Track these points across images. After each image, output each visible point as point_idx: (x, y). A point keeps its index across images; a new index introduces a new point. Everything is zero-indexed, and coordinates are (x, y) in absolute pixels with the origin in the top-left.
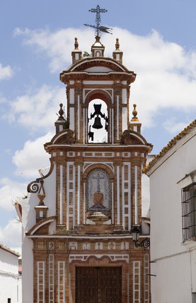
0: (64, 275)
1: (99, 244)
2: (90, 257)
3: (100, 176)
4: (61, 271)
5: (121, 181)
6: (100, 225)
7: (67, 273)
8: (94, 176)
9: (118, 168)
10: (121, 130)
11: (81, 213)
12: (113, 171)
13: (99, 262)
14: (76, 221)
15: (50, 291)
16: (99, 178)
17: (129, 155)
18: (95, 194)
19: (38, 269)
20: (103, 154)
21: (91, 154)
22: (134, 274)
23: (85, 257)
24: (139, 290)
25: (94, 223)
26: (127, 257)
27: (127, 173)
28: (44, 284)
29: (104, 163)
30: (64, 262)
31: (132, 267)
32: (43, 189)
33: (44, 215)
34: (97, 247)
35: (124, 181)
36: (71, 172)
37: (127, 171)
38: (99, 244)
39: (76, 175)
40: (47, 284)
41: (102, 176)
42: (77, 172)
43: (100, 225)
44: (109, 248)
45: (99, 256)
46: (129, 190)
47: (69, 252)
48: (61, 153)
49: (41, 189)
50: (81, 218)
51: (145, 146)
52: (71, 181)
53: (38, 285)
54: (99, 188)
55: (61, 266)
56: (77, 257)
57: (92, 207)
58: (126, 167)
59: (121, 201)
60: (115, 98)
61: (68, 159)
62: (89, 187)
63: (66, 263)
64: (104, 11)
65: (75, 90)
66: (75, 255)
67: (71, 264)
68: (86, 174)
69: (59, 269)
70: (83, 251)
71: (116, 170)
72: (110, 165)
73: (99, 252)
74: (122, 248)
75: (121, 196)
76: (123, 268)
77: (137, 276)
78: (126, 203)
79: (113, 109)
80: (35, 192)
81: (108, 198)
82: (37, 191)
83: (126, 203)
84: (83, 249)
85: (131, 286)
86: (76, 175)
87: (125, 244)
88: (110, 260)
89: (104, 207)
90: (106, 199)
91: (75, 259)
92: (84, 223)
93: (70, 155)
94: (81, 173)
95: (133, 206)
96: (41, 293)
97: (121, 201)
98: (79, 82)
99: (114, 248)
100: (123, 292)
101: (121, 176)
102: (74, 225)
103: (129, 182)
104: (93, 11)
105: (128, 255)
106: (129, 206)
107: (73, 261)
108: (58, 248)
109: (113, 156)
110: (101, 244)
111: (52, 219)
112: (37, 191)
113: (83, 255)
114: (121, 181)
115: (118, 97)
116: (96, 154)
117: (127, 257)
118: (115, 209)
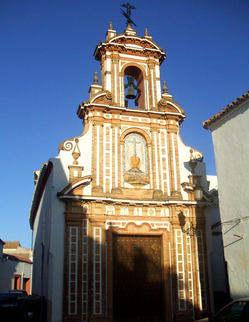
1: (138, 210)
2: (129, 224)
3: (136, 141)
5: (158, 146)
10: (156, 100)
11: (119, 176)
12: (150, 136)
13: (138, 230)
14: (114, 183)
15: (83, 262)
16: (135, 143)
17: (165, 122)
19: (71, 236)
20: (140, 119)
22: (177, 243)
23: (123, 224)
25: (132, 187)
26: (167, 225)
28: (77, 254)
29: (141, 128)
31: (174, 235)
32: (78, 147)
33: (78, 175)
34: (136, 213)
35: (161, 147)
36: (108, 134)
38: (138, 210)
39: (113, 137)
40: (80, 253)
41: (138, 141)
42: (114, 134)
43: (139, 189)
46: (166, 156)
48: (98, 114)
50: (119, 180)
52: (108, 142)
53: (70, 254)
54: (135, 151)
57: (129, 171)
58: (163, 133)
59: (159, 166)
60: (150, 72)
62: (126, 150)
64: (133, 8)
70: (121, 216)
71: (152, 135)
72: (147, 130)
74: (162, 214)
75: (159, 161)
76: (163, 236)
77: (179, 246)
78: (164, 168)
79: (147, 81)
80: (69, 150)
82: (71, 149)
83: (164, 168)
84: (121, 214)
86: (113, 137)
87: (165, 210)
88: (150, 227)
89: (141, 172)
90: (143, 163)
94: (119, 134)
95: (171, 172)
96: (73, 265)
97: (159, 166)
99: (154, 215)
101: (158, 142)
102: (111, 188)
103: (166, 148)
104: (124, 6)
105: (169, 223)
106: (167, 172)
109: (149, 122)
110: (141, 209)
112: (71, 149)
113: (121, 221)
114: (158, 146)
116: (132, 119)
117: (167, 225)
118: (154, 173)
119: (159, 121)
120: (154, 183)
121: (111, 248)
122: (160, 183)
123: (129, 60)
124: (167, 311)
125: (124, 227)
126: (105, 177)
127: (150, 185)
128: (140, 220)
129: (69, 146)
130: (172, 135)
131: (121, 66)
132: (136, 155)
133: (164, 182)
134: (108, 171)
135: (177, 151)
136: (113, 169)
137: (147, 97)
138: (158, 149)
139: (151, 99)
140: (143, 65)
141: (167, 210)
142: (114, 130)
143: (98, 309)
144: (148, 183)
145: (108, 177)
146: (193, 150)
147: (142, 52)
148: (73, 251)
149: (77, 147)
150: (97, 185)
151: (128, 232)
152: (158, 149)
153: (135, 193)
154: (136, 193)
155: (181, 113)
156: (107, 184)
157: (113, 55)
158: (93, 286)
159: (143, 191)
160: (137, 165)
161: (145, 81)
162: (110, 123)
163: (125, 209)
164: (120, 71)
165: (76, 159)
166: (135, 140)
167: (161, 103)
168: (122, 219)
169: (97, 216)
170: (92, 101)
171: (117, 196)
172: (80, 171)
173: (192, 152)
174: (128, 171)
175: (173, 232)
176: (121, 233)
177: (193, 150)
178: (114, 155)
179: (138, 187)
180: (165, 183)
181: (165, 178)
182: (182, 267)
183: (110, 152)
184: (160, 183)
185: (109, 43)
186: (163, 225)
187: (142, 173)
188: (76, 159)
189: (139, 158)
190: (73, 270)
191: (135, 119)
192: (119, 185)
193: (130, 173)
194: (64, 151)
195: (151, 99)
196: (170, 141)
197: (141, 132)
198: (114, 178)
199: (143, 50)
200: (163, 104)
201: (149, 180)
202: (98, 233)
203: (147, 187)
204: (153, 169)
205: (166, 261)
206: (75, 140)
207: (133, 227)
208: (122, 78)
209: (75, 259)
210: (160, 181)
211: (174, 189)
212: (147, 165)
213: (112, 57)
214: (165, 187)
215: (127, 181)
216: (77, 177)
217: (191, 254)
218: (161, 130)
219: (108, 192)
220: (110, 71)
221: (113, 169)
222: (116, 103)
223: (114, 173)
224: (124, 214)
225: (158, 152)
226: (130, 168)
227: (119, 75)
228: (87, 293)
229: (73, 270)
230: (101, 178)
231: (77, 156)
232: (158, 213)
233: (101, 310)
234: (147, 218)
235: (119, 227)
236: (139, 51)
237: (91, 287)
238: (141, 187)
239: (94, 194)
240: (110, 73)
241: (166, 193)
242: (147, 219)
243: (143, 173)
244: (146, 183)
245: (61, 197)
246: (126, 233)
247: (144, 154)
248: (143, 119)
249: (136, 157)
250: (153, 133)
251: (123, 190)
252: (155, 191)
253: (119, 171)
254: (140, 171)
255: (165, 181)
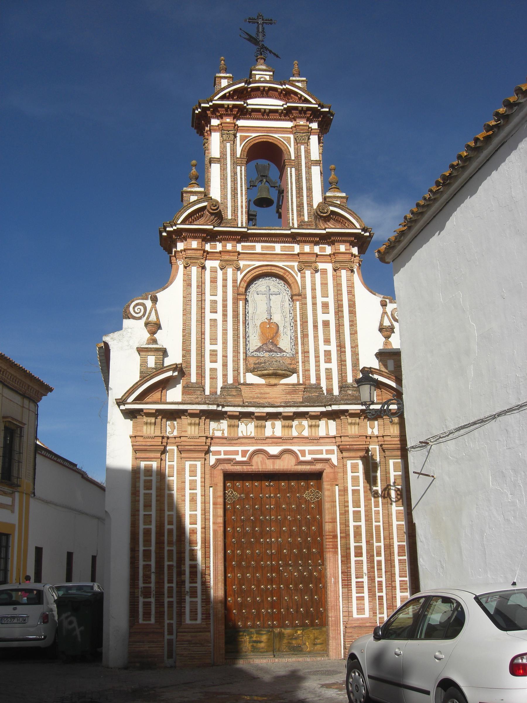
0: (199, 491)
4: (193, 484)
5: (314, 297)
6: (275, 385)
7: (204, 486)
8: (260, 289)
9: (308, 273)
10: (310, 204)
12: (299, 279)
13: (274, 464)
14: (225, 376)
15: (167, 527)
16: (269, 294)
17: (329, 250)
18: (263, 323)
20: (278, 248)
21: (254, 247)
22: (350, 488)
23: (244, 453)
24: (363, 523)
25: (262, 381)
27: (327, 284)
28: (153, 513)
29: (280, 264)
30: (199, 464)
31: (345, 472)
32: (156, 311)
34: (268, 432)
35: (320, 300)
36: (214, 281)
37: (326, 279)
39: (225, 286)
41: (276, 290)
42: (225, 280)
43: (275, 385)
44: (295, 433)
45: (274, 450)
46: (331, 317)
47: (209, 440)
48: (194, 244)
49: (151, 311)
50: (236, 370)
51: (360, 231)
52: (213, 298)
53: (142, 513)
55: (193, 473)
56: (226, 453)
57: (258, 350)
58: (324, 272)
59: (316, 337)
61: (206, 255)
63: (204, 465)
64: (270, 22)
65: (222, 136)
66: (222, 449)
67: (214, 467)
68: (244, 285)
69: (188, 478)
71: (303, 277)
72: (292, 267)
73: (275, 440)
74: (322, 432)
75: (315, 327)
78: (327, 341)
79: (293, 169)
80: (140, 318)
81: (289, 333)
82: (144, 315)
83: (327, 341)
84: (240, 435)
85: (345, 513)
86: (225, 286)
87: (327, 424)
89: (281, 351)
91: (222, 456)
92: (242, 382)
93: (211, 248)
94: (235, 281)
96: (147, 532)
97: (316, 337)
98: (228, 120)
99: (306, 433)
100: (327, 527)
101: (314, 289)
102: (220, 384)
103: (331, 300)
104: (252, 21)
105: (335, 448)
106: (333, 347)
107: (218, 460)
108: (186, 431)
110: (278, 424)
111: (174, 370)
112: (144, 315)
113: (240, 449)
114: (314, 297)
115: (302, 147)
116: (262, 247)
118: (306, 353)
119: (317, 249)
120: (307, 371)
121: (221, 500)
122: (318, 370)
123: (257, 131)
124: (330, 619)
125: (245, 459)
126: (208, 365)
127: (298, 376)
128: (276, 444)
129: (139, 310)
130: (344, 273)
131: (241, 145)
132: (271, 319)
133: (326, 369)
134: (214, 353)
135: (352, 305)
136: (225, 348)
137: (292, 202)
138: (314, 304)
139: (300, 206)
140: (284, 137)
141: (332, 424)
142: (225, 274)
143: (194, 612)
144: (294, 371)
145: (213, 365)
146: (386, 300)
147: (282, 112)
148: (147, 506)
149: (153, 312)
150: (192, 382)
151: (253, 467)
152: (314, 304)
153: (267, 394)
154: (269, 393)
155: (359, 229)
156: (213, 378)
157: (223, 125)
158: (185, 570)
159: (284, 387)
160: (272, 338)
161: (289, 169)
162: (217, 260)
163: (246, 425)
164: (238, 156)
165: (153, 333)
166: (270, 289)
167: (319, 213)
168: (242, 444)
169: (191, 440)
170: (179, 222)
171: (230, 399)
172: (158, 357)
173: (386, 305)
174: (256, 351)
175: (345, 466)
176: (239, 470)
177: (386, 300)
178: (225, 321)
179: (273, 381)
180: (329, 372)
181: (328, 360)
182: (361, 535)
183: (219, 316)
184: (318, 370)
185: (214, 102)
186: (324, 452)
187: (282, 353)
188: (153, 333)
189: (276, 324)
190: (147, 542)
191: (267, 248)
192: (236, 378)
193: (258, 353)
194: (131, 320)
195: (300, 206)
196: (338, 286)
197: (281, 272)
198: (225, 365)
199: (282, 108)
200: (322, 214)
201: (295, 366)
202: (193, 471)
203: (293, 379)
204: (303, 344)
205: (330, 522)
206: (151, 297)
207: (263, 458)
208: (243, 167)
209: (151, 522)
210: (318, 366)
211: (346, 381)
212: (293, 337)
213: (221, 128)
214: (329, 378)
215: (252, 371)
216: (153, 368)
217: (380, 509)
218: (321, 266)
219: (213, 393)
220: (219, 157)
221: (225, 348)
222: (230, 220)
223: (225, 356)
224: (245, 434)
225: (315, 310)
226: (260, 344)
227: (235, 164)
228: (174, 585)
229: (147, 542)
230: (201, 367)
231: (153, 329)
232: (313, 429)
233: (199, 616)
234: (291, 440)
235: (234, 459)
236: (276, 111)
237: (181, 573)
238: (280, 381)
239: (187, 398)
240: (217, 160)
241: (330, 391)
242: (291, 441)
243: (285, 352)
244: (289, 373)
245: (123, 407)
246: (250, 470)
247: (288, 315)
248: (284, 246)
249: (271, 321)
250: (305, 273)
251: (242, 387)
252: (307, 388)
253: (236, 351)
254: (279, 348)
255: (328, 366)
